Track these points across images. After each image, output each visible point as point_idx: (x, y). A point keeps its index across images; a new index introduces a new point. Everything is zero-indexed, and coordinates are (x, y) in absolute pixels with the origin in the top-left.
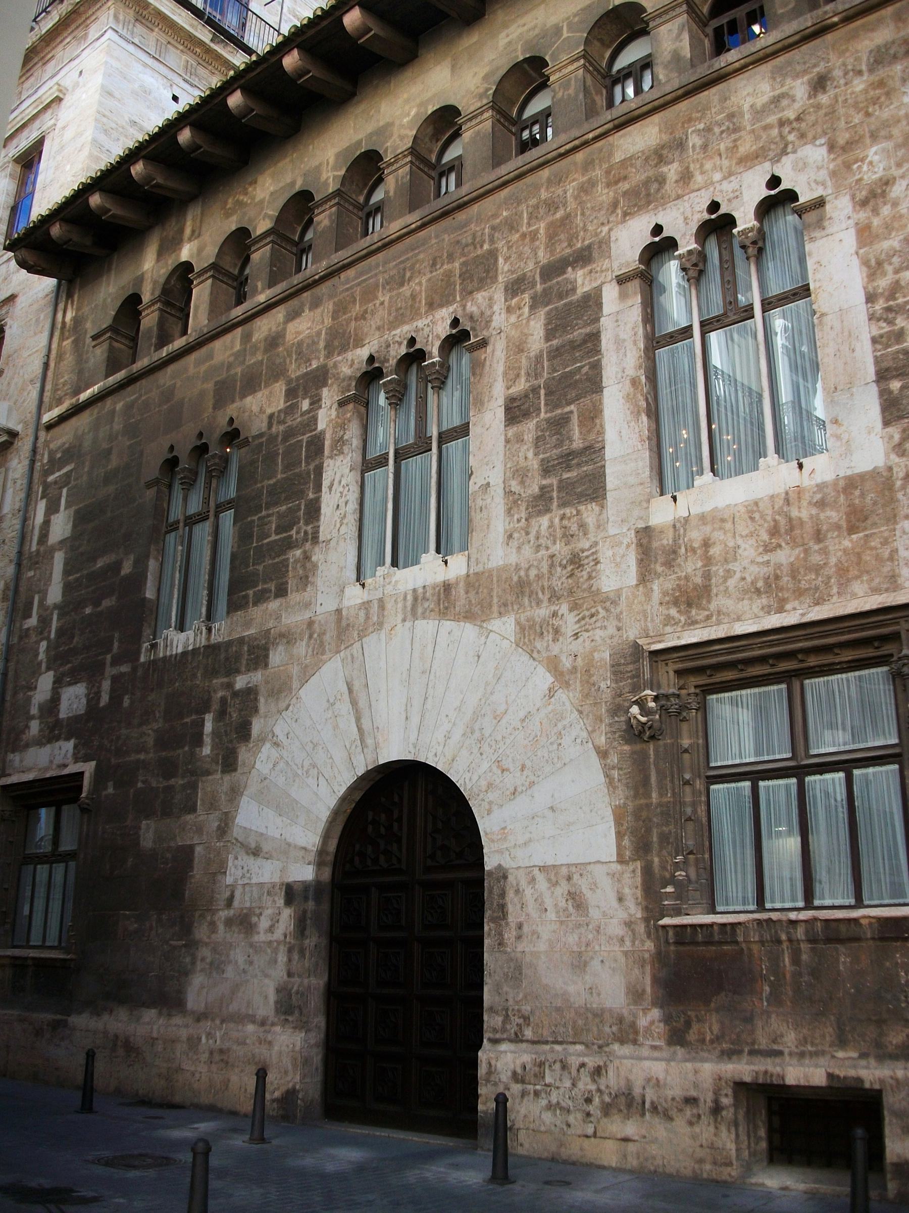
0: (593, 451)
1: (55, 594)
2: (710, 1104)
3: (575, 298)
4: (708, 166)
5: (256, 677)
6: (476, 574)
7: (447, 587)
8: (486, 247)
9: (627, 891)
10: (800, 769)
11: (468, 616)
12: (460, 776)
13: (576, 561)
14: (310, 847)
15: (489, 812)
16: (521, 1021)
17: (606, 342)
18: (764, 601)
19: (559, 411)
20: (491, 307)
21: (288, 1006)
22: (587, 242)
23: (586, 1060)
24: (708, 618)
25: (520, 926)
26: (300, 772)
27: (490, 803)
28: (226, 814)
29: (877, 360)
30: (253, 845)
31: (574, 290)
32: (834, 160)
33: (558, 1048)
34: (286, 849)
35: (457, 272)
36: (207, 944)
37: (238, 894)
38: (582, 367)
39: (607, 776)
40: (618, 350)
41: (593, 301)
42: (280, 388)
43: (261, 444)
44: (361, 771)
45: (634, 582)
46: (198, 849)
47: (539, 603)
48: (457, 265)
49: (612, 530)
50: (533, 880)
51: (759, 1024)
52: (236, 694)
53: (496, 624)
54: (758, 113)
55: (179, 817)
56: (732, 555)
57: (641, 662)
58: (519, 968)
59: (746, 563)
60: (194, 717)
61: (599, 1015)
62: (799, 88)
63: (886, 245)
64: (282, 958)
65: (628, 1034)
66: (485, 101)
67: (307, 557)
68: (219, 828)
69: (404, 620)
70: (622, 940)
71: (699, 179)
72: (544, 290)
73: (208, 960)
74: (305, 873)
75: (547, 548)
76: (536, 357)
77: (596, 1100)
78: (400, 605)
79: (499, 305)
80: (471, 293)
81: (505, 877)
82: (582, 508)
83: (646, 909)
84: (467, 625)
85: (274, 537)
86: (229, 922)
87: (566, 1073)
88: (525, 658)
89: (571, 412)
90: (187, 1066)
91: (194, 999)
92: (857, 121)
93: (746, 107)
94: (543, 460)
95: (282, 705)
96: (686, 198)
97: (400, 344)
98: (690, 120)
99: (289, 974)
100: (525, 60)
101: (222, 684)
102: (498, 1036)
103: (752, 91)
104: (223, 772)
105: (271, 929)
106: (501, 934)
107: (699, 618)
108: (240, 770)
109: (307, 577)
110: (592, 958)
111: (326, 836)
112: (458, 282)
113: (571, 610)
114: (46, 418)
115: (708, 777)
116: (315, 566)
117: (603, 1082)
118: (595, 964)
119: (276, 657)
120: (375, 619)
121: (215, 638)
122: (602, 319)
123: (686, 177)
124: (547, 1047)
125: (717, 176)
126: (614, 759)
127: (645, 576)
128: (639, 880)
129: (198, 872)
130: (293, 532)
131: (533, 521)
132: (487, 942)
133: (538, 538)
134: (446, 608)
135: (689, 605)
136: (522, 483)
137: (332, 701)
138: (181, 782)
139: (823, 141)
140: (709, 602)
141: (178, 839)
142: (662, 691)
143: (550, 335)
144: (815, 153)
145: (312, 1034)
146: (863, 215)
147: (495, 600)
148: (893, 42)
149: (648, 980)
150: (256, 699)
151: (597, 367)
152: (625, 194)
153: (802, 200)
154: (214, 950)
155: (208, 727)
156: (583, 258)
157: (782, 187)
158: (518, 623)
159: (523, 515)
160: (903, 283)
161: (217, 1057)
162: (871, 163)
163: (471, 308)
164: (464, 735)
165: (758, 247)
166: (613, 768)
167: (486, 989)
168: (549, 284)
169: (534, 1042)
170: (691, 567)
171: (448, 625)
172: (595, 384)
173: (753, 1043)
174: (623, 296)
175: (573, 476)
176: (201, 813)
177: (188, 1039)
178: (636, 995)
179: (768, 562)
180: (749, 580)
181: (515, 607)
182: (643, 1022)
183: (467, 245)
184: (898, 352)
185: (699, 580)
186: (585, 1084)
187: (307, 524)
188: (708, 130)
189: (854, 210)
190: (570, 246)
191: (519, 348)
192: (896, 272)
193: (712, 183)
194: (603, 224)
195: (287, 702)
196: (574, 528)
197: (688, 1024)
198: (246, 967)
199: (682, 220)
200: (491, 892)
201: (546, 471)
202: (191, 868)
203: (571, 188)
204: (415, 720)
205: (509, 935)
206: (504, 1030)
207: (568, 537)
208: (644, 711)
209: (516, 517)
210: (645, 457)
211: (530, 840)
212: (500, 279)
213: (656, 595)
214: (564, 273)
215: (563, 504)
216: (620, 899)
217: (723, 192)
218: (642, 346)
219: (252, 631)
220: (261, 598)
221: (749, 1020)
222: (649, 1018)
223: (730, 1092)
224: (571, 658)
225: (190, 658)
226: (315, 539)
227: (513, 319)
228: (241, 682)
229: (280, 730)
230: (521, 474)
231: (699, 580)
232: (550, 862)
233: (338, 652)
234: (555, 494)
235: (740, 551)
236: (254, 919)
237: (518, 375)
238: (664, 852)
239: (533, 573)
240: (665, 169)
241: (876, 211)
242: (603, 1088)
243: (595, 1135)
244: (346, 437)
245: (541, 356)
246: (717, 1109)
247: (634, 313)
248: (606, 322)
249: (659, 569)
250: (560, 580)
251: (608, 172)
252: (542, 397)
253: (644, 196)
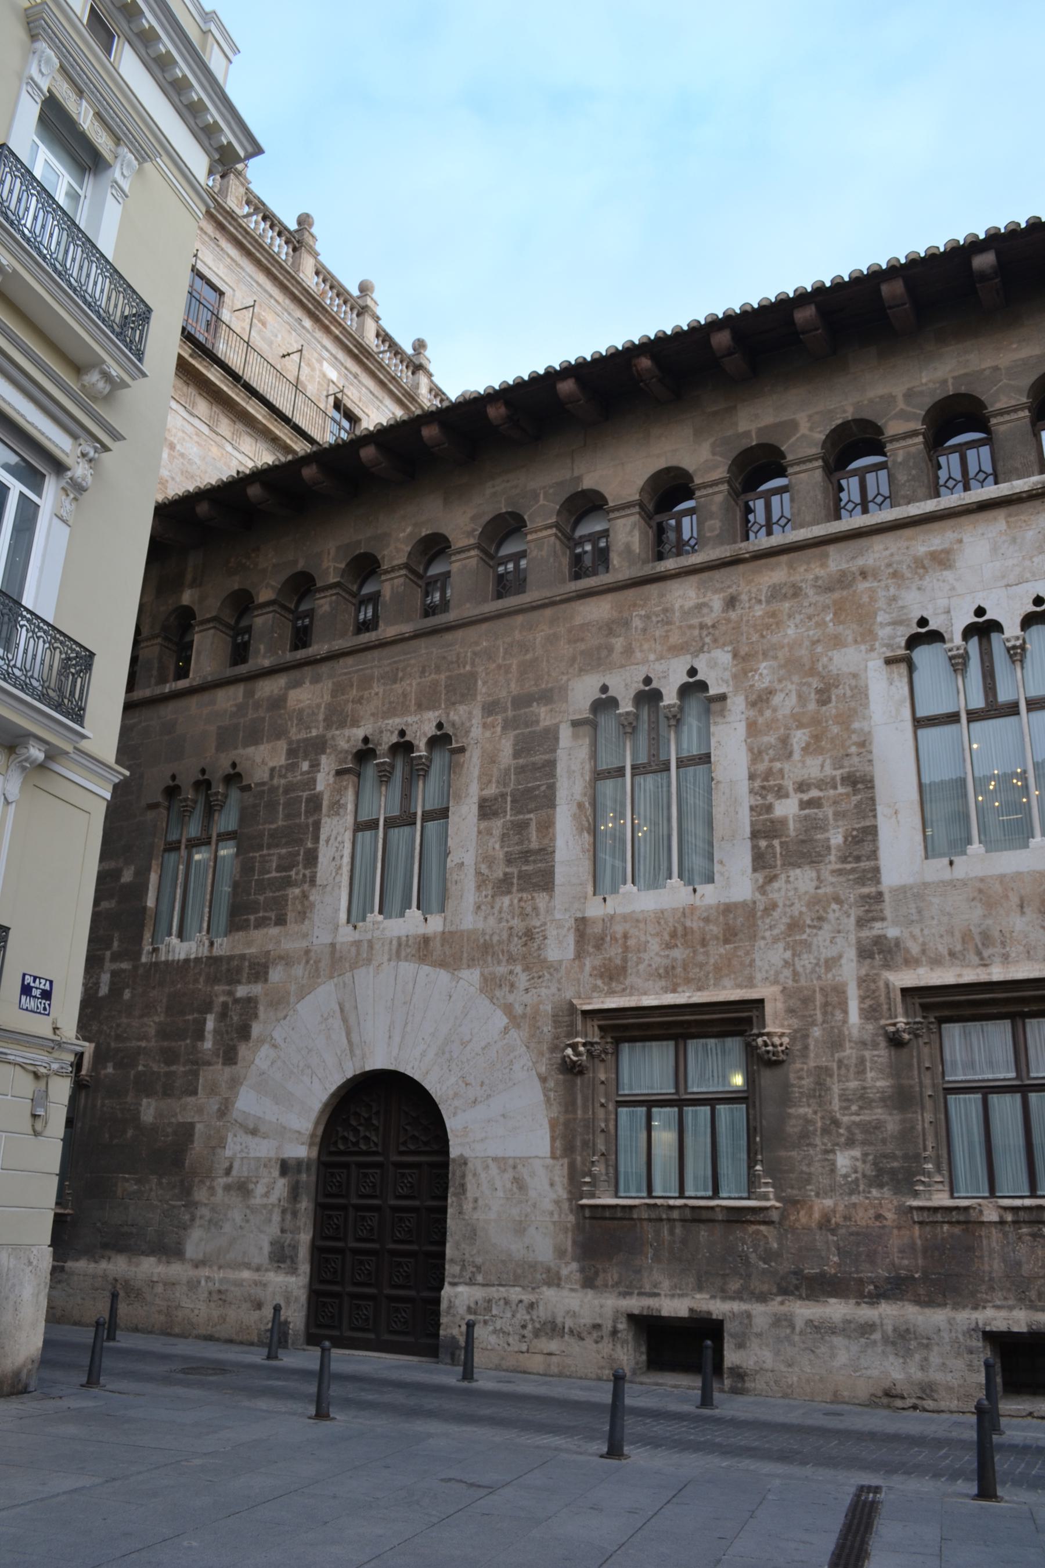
0: (546, 853)
2: (610, 1328)
3: (538, 728)
4: (646, 646)
5: (256, 989)
6: (451, 933)
7: (426, 940)
8: (468, 668)
9: (557, 1179)
10: (679, 1103)
11: (442, 964)
12: (430, 1085)
13: (529, 935)
14: (303, 1131)
15: (455, 1114)
16: (474, 1269)
17: (561, 769)
18: (663, 983)
19: (521, 817)
20: (470, 720)
21: (281, 1256)
22: (550, 685)
23: (523, 1297)
24: (624, 990)
25: (476, 1200)
26: (295, 1070)
27: (456, 1108)
28: (227, 1099)
29: (753, 824)
30: (251, 1126)
31: (537, 722)
32: (736, 665)
33: (502, 1289)
34: (282, 1131)
35: (443, 683)
36: (206, 1205)
37: (236, 1165)
38: (540, 786)
39: (545, 1095)
40: (569, 778)
41: (550, 736)
42: (282, 746)
43: (263, 792)
44: (350, 1074)
45: (572, 957)
46: (199, 1127)
47: (499, 962)
48: (443, 676)
49: (558, 916)
50: (487, 1167)
51: (645, 1274)
52: (236, 1001)
53: (465, 974)
54: (686, 613)
55: (180, 1099)
56: (642, 948)
57: (572, 1016)
58: (474, 1232)
59: (652, 954)
60: (196, 1015)
61: (533, 1266)
62: (717, 602)
63: (766, 739)
64: (276, 1217)
65: (554, 1280)
66: (472, 541)
67: (305, 896)
68: (219, 1110)
69: (390, 960)
70: (552, 1214)
71: (639, 655)
72: (514, 716)
73: (207, 1218)
74: (300, 1151)
75: (507, 921)
76: (505, 769)
77: (530, 1327)
78: (386, 948)
79: (477, 720)
80: (454, 704)
81: (465, 1164)
82: (536, 895)
83: (570, 1192)
84: (442, 971)
85: (274, 874)
86: (227, 1188)
87: (508, 1307)
88: (487, 1002)
89: (531, 819)
90: (186, 1303)
91: (191, 1250)
92: (754, 639)
93: (677, 606)
94: (507, 852)
95: (281, 1015)
96: (628, 668)
97: (392, 732)
98: (635, 605)
99: (283, 1231)
100: (507, 513)
101: (223, 991)
102: (456, 1280)
103: (683, 595)
104: (224, 1064)
105: (267, 1195)
106: (461, 1206)
107: (617, 989)
108: (240, 1064)
109: (305, 913)
110: (529, 1226)
111: (317, 1123)
112: (444, 692)
113: (524, 971)
115: (617, 1102)
116: (312, 905)
117: (534, 1313)
118: (532, 1230)
119: (276, 975)
120: (365, 955)
121: (217, 952)
122: (559, 751)
123: (628, 651)
124: (494, 1289)
125: (652, 657)
126: (551, 1084)
127: (579, 955)
128: (565, 1171)
129: (198, 1145)
130: (293, 873)
131: (497, 899)
132: (450, 1211)
133: (500, 912)
134: (425, 955)
135: (611, 979)
136: (490, 867)
137: (325, 1016)
138: (182, 1069)
139: (729, 648)
140: (625, 979)
141: (179, 1117)
142: (589, 1040)
143: (516, 755)
144: (723, 657)
145: (301, 1278)
146: (752, 713)
147: (465, 955)
148: (785, 584)
149: (569, 1243)
150: (256, 1007)
151: (552, 787)
152: (582, 653)
153: (712, 691)
154: (213, 1210)
155: (210, 1024)
156: (546, 697)
157: (698, 678)
158: (482, 974)
159: (490, 892)
160: (774, 770)
161: (215, 1297)
162: (761, 674)
163: (453, 716)
164: (436, 1054)
165: (676, 720)
166: (551, 1090)
167: (448, 1245)
168: (518, 712)
169: (484, 1285)
170: (614, 951)
171: (426, 969)
172: (550, 802)
173: (641, 1288)
174: (575, 736)
175: (528, 870)
176: (202, 1097)
177: (188, 1282)
178: (561, 1253)
179: (668, 956)
180: (654, 966)
181: (481, 963)
182: (564, 1272)
183: (452, 662)
184: (766, 820)
185: (618, 962)
186: (522, 1315)
187: (305, 868)
188: (648, 617)
189: (746, 708)
190: (536, 685)
191: (490, 759)
192: (771, 761)
193: (648, 661)
194: (563, 673)
195: (285, 1013)
196: (529, 909)
197: (597, 1273)
198: (243, 1224)
199: (624, 686)
200: (454, 1174)
201: (509, 861)
202: (192, 1142)
203: (539, 637)
204: (397, 1039)
205: (468, 1207)
206: (461, 1276)
207: (524, 915)
208: (577, 1054)
209: (484, 893)
210: (586, 865)
211: (486, 1138)
212: (479, 698)
213: (588, 968)
214: (531, 706)
215: (521, 890)
216: (552, 1185)
217: (655, 670)
218: (588, 779)
219: (253, 950)
220: (261, 924)
221: (638, 1272)
222: (569, 1269)
223: (624, 1320)
224: (522, 1007)
225: (192, 964)
226: (313, 881)
227: (488, 734)
228: (241, 991)
229: (278, 1035)
230: (488, 859)
231: (618, 962)
232: (500, 1154)
233: (332, 977)
234: (515, 881)
235: (649, 945)
236: (251, 1186)
237: (490, 782)
238: (585, 1153)
239: (495, 938)
240: (613, 640)
241: (761, 712)
242: (535, 1317)
243: (528, 1352)
244: (342, 802)
245: (509, 769)
246: (614, 1332)
247: (583, 752)
248: (561, 755)
249: (591, 950)
250: (516, 947)
251: (570, 631)
252: (509, 803)
253: (596, 659)
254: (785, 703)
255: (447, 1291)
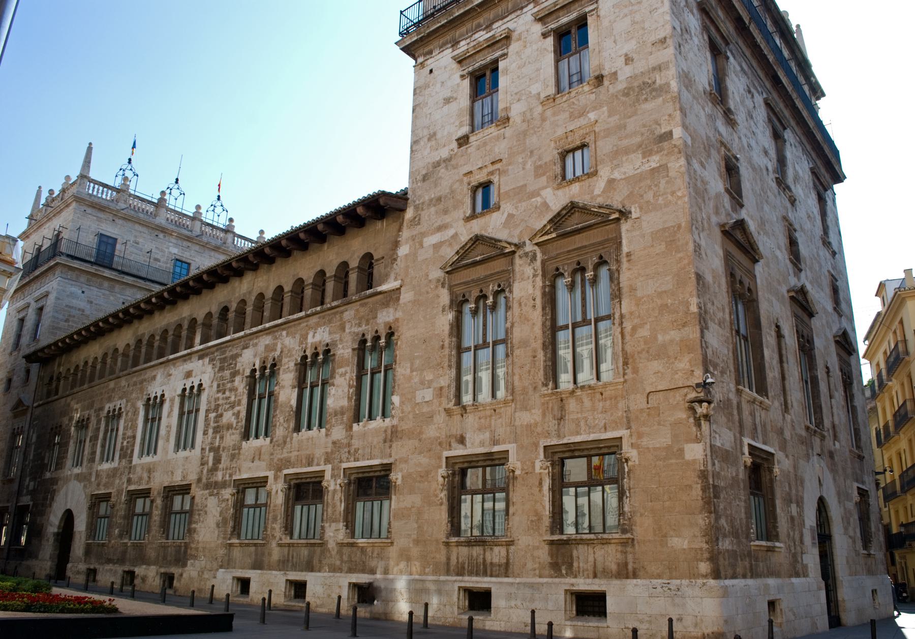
1: (31, 457)
74: (56, 530)
91: (40, 557)
111: (60, 522)
114: (35, 405)
253: (110, 400)
254: (130, 414)
255: (69, 565)
